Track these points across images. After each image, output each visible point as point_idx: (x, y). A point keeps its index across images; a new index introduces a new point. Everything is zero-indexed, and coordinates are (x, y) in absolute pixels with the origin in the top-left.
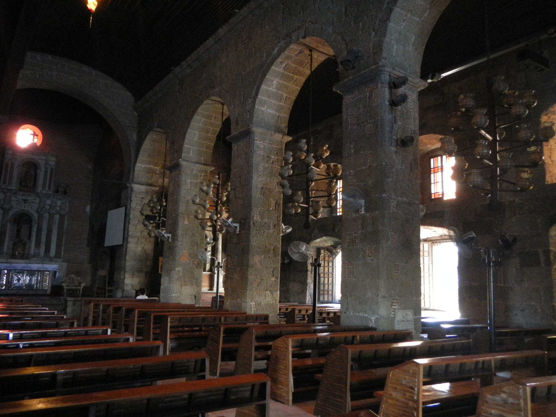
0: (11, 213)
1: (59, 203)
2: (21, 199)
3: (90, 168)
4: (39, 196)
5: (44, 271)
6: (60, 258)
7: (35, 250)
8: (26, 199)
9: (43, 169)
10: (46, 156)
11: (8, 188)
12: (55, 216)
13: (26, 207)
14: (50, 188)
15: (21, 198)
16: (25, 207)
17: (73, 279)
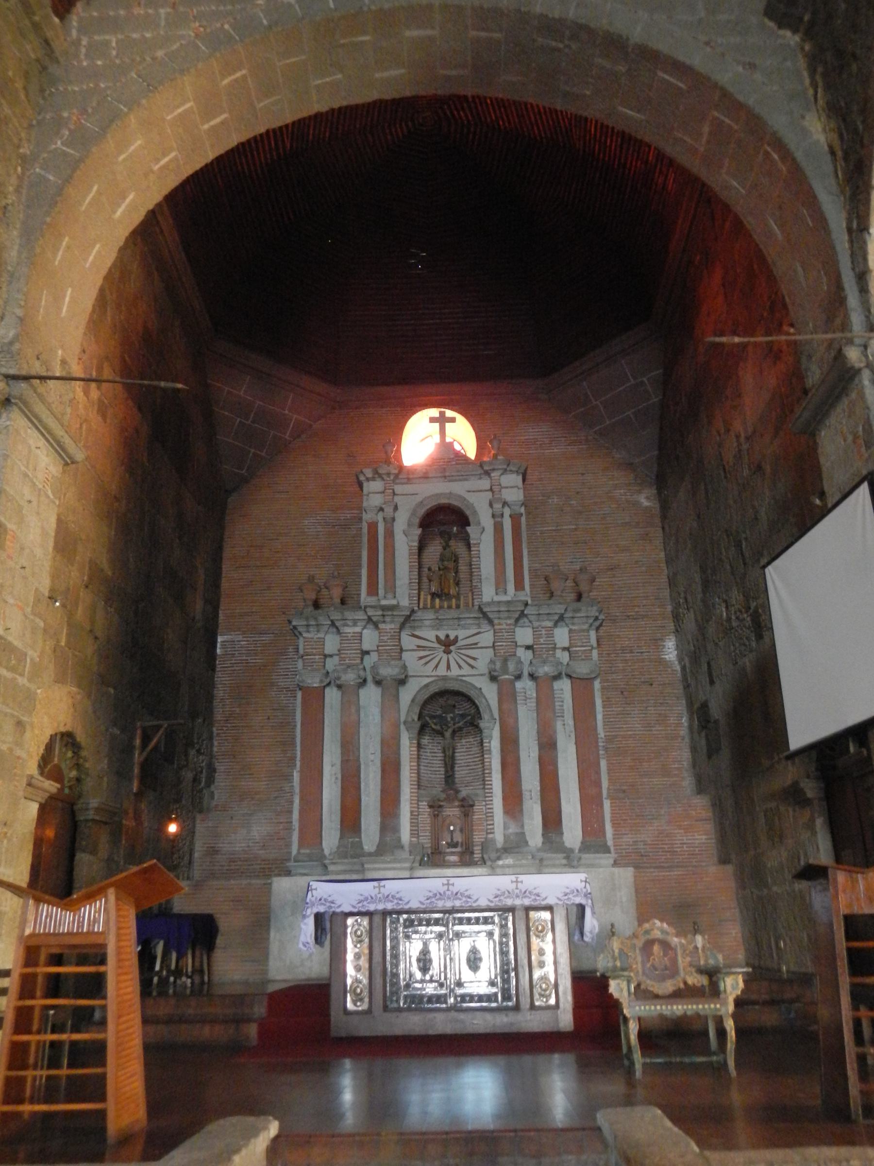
0: (407, 695)
1: (562, 636)
2: (434, 640)
3: (646, 503)
4: (491, 622)
5: (528, 909)
6: (607, 850)
7: (506, 827)
8: (447, 636)
9: (487, 522)
10: (487, 473)
11: (384, 602)
12: (557, 685)
13: (453, 664)
14: (519, 585)
15: (430, 634)
16: (448, 667)
17: (665, 945)
